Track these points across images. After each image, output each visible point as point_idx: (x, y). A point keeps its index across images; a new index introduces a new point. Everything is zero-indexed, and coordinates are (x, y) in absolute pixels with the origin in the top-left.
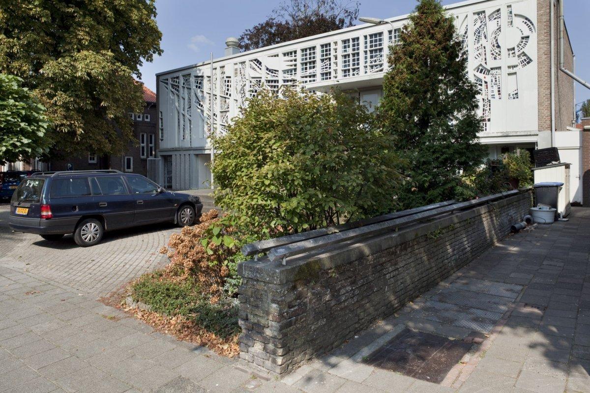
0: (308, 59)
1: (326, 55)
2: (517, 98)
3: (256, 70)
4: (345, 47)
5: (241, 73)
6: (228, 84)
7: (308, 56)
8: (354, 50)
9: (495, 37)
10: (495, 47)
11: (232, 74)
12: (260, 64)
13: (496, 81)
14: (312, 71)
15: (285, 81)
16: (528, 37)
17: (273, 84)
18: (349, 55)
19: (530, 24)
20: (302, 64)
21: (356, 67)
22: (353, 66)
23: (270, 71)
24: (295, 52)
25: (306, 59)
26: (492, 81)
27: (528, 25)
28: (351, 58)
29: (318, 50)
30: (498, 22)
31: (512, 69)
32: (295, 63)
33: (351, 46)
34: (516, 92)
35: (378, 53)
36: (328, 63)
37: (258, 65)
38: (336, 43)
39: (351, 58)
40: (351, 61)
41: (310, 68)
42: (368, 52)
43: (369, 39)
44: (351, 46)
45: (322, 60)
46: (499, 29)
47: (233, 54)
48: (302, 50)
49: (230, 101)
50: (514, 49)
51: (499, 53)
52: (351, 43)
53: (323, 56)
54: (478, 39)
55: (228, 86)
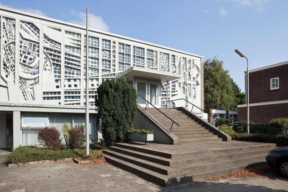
5: (5, 28)
13: (189, 89)
15: (66, 54)
18: (123, 54)
41: (92, 52)
46: (190, 68)
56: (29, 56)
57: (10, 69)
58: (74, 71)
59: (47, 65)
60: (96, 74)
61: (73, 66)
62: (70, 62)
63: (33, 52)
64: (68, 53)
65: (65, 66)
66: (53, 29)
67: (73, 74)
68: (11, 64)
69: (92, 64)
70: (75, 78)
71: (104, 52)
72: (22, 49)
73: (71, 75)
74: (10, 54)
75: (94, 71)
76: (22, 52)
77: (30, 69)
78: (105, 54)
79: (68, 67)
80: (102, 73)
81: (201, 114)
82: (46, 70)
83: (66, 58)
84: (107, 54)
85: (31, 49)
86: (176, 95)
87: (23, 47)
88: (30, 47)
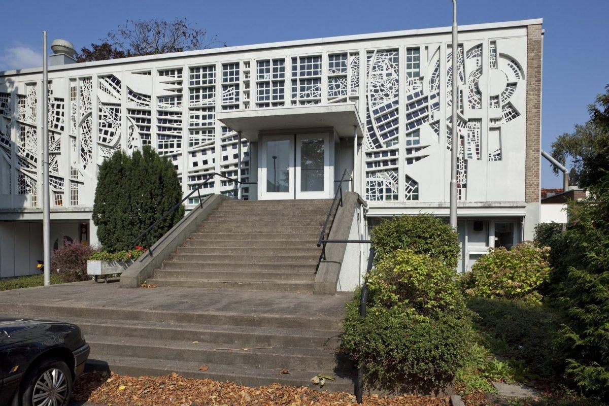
0: (201, 83)
1: (231, 80)
2: (500, 159)
3: (109, 93)
4: (261, 71)
5: (82, 95)
6: (58, 110)
7: (201, 79)
8: (275, 76)
9: (474, 80)
10: (474, 93)
11: (66, 96)
12: (118, 83)
13: (474, 136)
14: (207, 101)
15: (160, 113)
16: (515, 84)
17: (141, 116)
18: (267, 83)
19: (517, 69)
20: (191, 90)
21: (278, 100)
22: (273, 99)
23: (135, 96)
24: (180, 71)
25: (198, 83)
26: (469, 137)
27: (514, 69)
28: (271, 88)
29: (219, 71)
30: (478, 60)
31: (493, 122)
32: (179, 87)
33: (271, 70)
34: (499, 152)
35: (312, 85)
36: (234, 91)
37: (114, 85)
38: (247, 64)
39: (271, 88)
40: (271, 92)
41: (205, 97)
42: (298, 82)
43: (299, 64)
44: (271, 70)
45: (225, 87)
46: (480, 70)
47: (65, 63)
48: (192, 69)
49: (63, 138)
50: (497, 97)
51: (478, 100)
52: (271, 67)
53: (225, 80)
54: (452, 81)
55: (58, 113)
56: (110, 130)
57: (88, 155)
58: (173, 141)
59: (133, 139)
60: (211, 139)
61: (172, 131)
62: (168, 125)
63: (115, 121)
64: (164, 109)
65: (159, 135)
66: (142, 75)
67: (172, 146)
68: (89, 148)
69: (204, 121)
70: (175, 153)
71: (226, 91)
72: (102, 121)
73: (169, 150)
74: (89, 133)
75: (207, 134)
76: (101, 125)
77: (111, 150)
78: (230, 95)
79: (164, 136)
80: (223, 135)
81: (524, 207)
82: (131, 147)
83: (160, 120)
84: (233, 93)
85: (112, 117)
86: (425, 157)
87: (102, 117)
88: (111, 115)
